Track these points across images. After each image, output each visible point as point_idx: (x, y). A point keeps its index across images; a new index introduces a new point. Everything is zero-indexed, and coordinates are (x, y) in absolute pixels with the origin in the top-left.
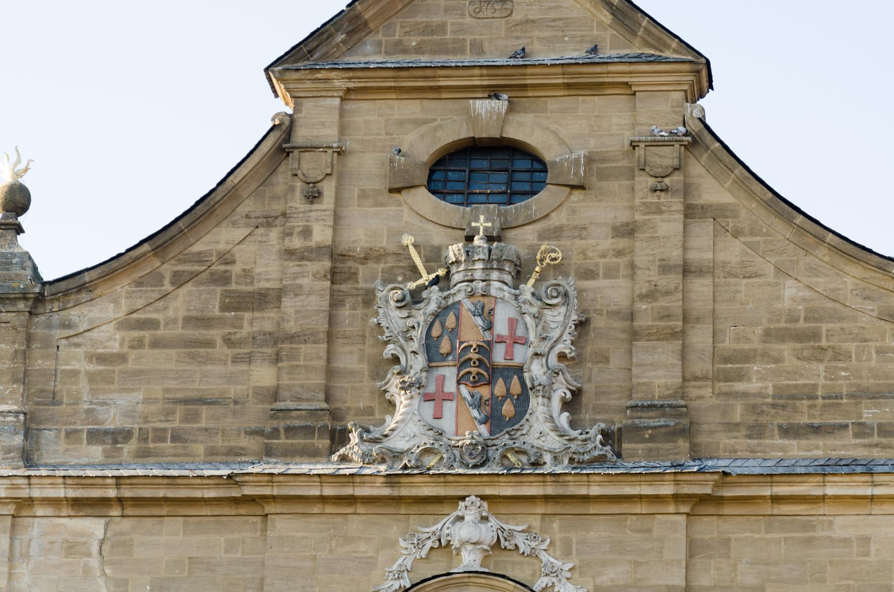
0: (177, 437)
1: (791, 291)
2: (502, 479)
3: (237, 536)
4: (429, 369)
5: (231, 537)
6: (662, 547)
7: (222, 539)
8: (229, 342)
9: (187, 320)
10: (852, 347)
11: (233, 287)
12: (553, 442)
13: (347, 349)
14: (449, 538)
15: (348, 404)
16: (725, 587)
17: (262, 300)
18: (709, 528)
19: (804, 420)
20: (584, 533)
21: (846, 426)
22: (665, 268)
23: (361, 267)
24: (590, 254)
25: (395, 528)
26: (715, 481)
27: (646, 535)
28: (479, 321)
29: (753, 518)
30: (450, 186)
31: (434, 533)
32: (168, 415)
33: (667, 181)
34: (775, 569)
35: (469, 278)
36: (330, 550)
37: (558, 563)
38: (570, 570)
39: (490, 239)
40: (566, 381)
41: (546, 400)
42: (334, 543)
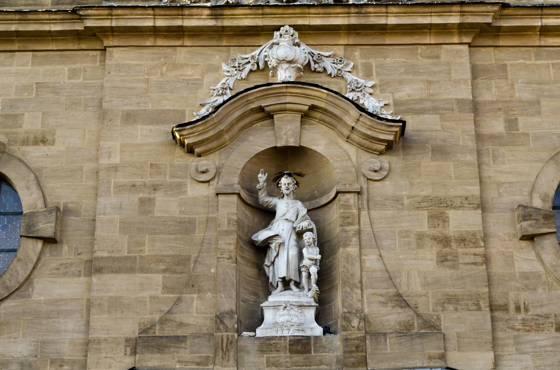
2: (312, 10)
3: (78, 66)
5: (74, 66)
6: (450, 70)
7: (66, 69)
14: (266, 59)
16: (506, 101)
18: (488, 57)
20: (382, 59)
25: (218, 57)
26: (495, 12)
27: (435, 60)
29: (523, 49)
31: (253, 57)
34: (547, 87)
36: (162, 75)
37: (362, 81)
38: (372, 87)
42: (164, 69)
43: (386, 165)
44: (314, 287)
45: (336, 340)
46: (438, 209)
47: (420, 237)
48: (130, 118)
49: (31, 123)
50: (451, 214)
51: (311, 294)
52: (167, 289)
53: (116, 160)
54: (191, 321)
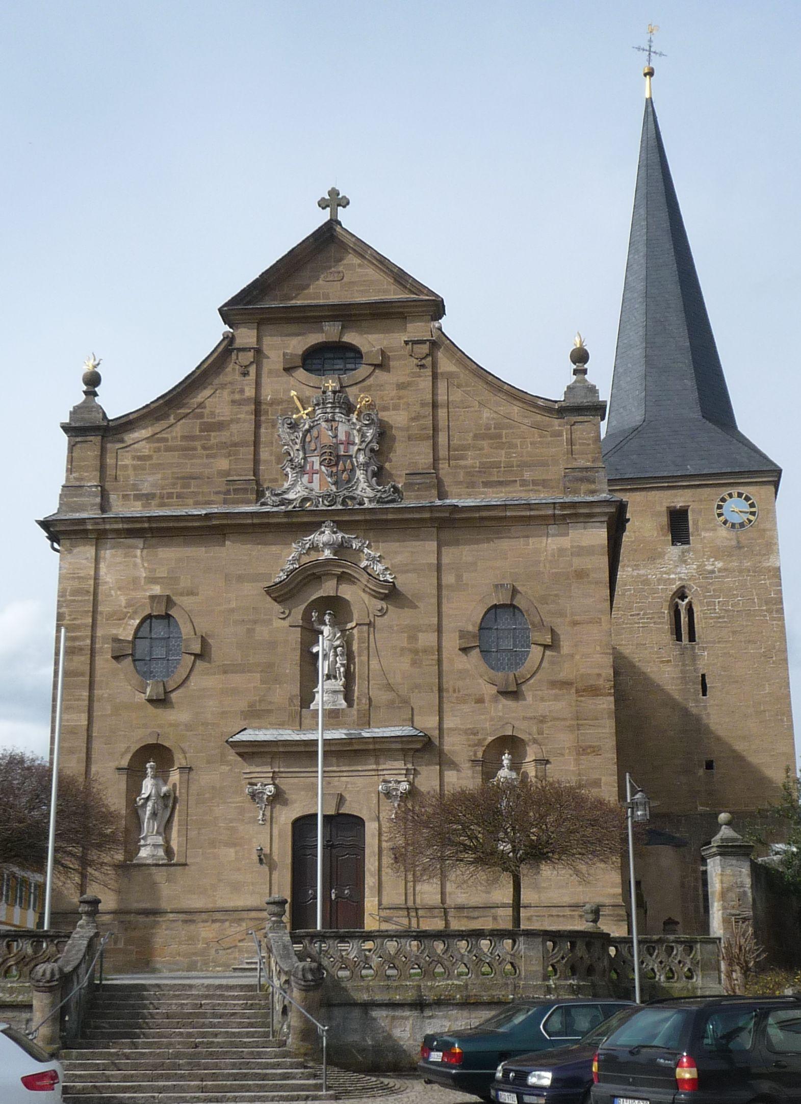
0: (179, 496)
1: (486, 414)
4: (305, 458)
8: (204, 448)
9: (184, 438)
10: (518, 441)
11: (206, 420)
12: (370, 493)
17: (220, 426)
19: (496, 479)
21: (516, 481)
22: (423, 405)
23: (270, 409)
24: (385, 398)
28: (330, 433)
30: (314, 367)
32: (174, 484)
33: (423, 361)
39: (334, 392)
43: (385, 606)
44: (343, 679)
45: (354, 711)
46: (413, 633)
47: (402, 649)
48: (240, 578)
49: (185, 582)
50: (420, 635)
51: (341, 683)
52: (263, 682)
53: (233, 605)
54: (276, 700)
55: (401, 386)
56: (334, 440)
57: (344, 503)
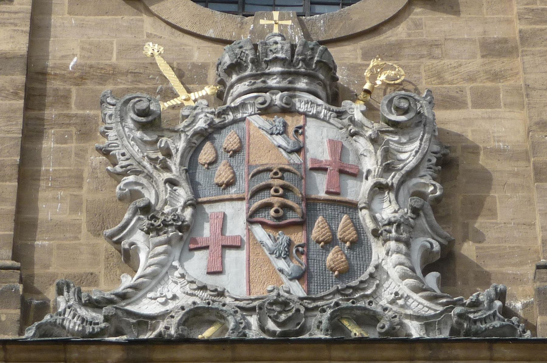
4: (195, 204)
13: (49, 194)
15: (51, 270)
24: (448, 76)
28: (279, 140)
35: (261, 85)
40: (431, 227)
41: (402, 247)
55: (495, 49)
56: (296, 159)
57: (335, 324)
